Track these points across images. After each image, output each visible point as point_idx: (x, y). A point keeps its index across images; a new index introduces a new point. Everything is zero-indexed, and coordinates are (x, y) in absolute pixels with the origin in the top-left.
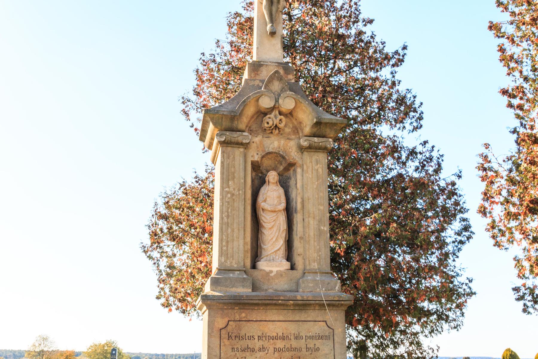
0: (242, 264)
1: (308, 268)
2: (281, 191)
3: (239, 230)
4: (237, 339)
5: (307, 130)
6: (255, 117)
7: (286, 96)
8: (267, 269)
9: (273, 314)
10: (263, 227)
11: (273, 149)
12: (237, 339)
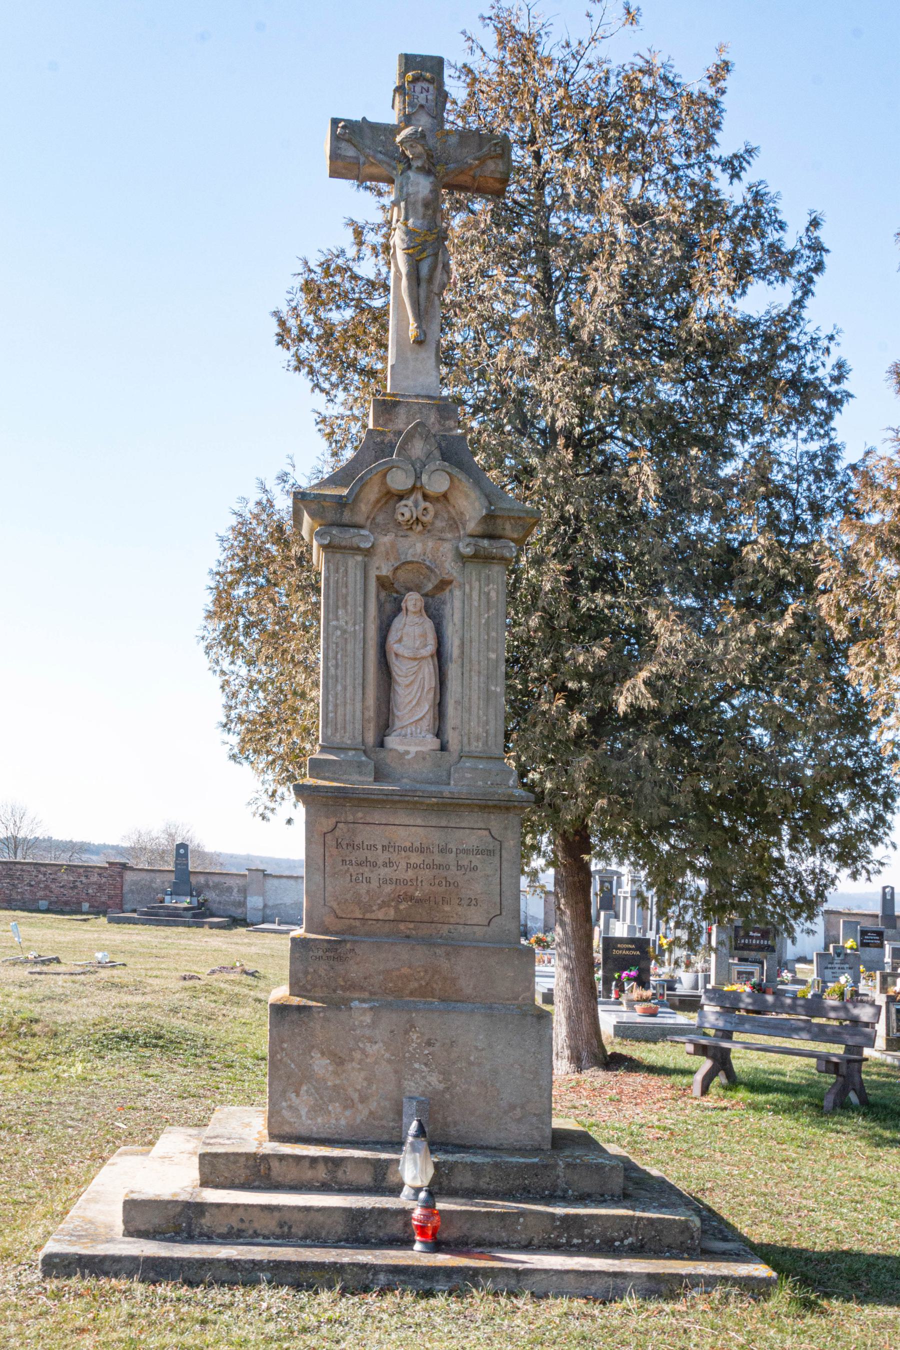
0: (360, 739)
1: (466, 749)
2: (429, 624)
3: (354, 687)
4: (350, 848)
5: (472, 526)
6: (384, 500)
7: (433, 468)
8: (401, 748)
9: (402, 818)
10: (397, 682)
11: (413, 556)
12: (350, 848)
